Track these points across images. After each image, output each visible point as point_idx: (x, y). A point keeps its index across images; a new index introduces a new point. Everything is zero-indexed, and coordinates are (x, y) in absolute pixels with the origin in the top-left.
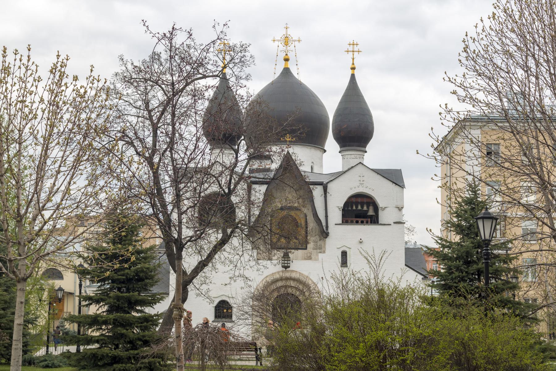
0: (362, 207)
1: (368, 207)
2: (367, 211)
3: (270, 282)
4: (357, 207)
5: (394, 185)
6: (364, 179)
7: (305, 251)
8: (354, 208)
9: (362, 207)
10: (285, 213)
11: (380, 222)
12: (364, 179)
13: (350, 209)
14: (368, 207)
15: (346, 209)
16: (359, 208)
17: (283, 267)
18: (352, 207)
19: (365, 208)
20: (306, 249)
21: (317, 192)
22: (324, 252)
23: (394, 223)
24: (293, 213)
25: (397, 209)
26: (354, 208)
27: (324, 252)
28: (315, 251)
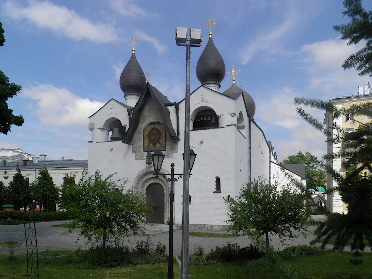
0: (207, 118)
1: (211, 118)
2: (211, 120)
3: (141, 175)
4: (203, 119)
5: (227, 98)
6: (204, 96)
7: (165, 151)
8: (202, 119)
9: (207, 118)
10: (152, 126)
11: (219, 127)
12: (204, 96)
13: (199, 120)
14: (211, 118)
15: (197, 121)
16: (205, 119)
17: (147, 163)
18: (200, 119)
19: (209, 119)
20: (165, 150)
21: (172, 109)
22: (177, 152)
23: (227, 126)
24: (157, 126)
25: (230, 115)
26: (202, 119)
27: (177, 152)
28: (171, 151)
